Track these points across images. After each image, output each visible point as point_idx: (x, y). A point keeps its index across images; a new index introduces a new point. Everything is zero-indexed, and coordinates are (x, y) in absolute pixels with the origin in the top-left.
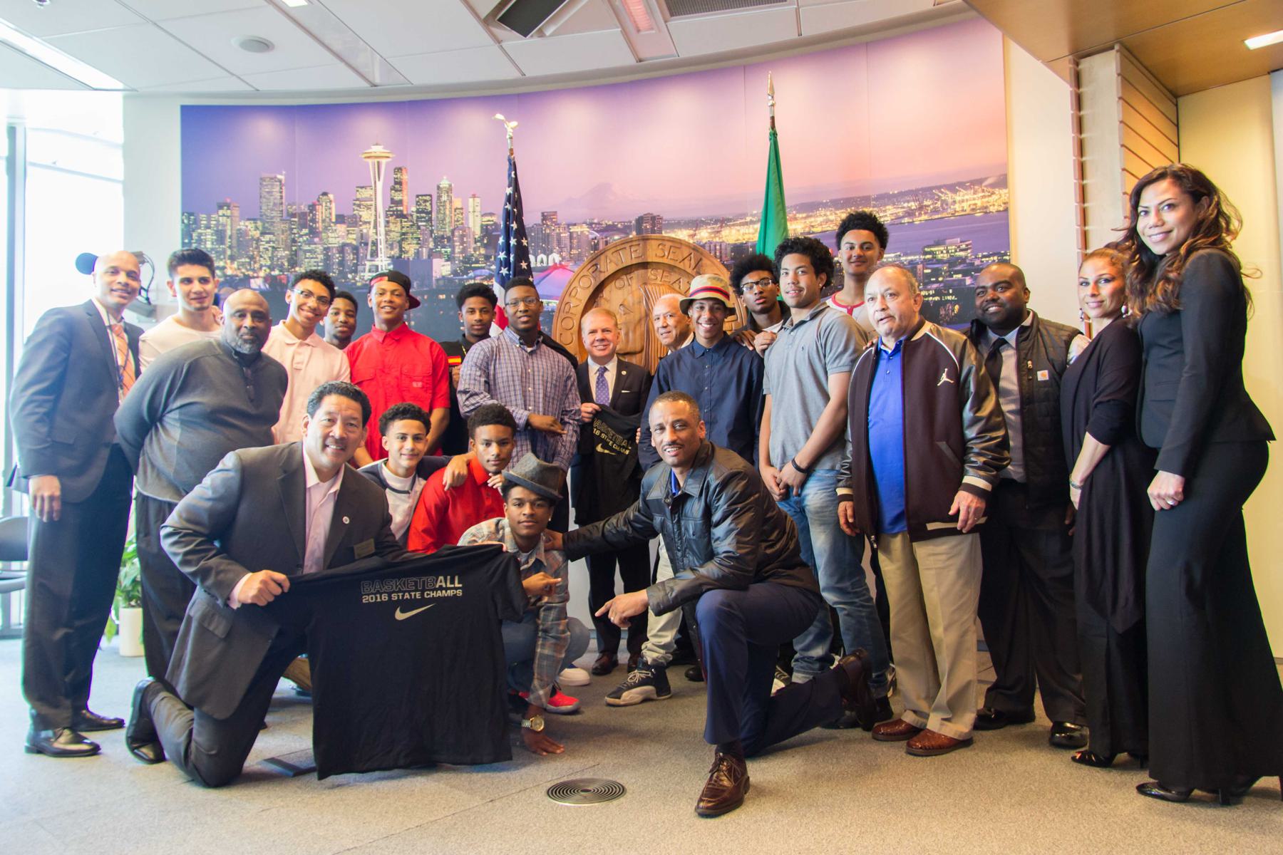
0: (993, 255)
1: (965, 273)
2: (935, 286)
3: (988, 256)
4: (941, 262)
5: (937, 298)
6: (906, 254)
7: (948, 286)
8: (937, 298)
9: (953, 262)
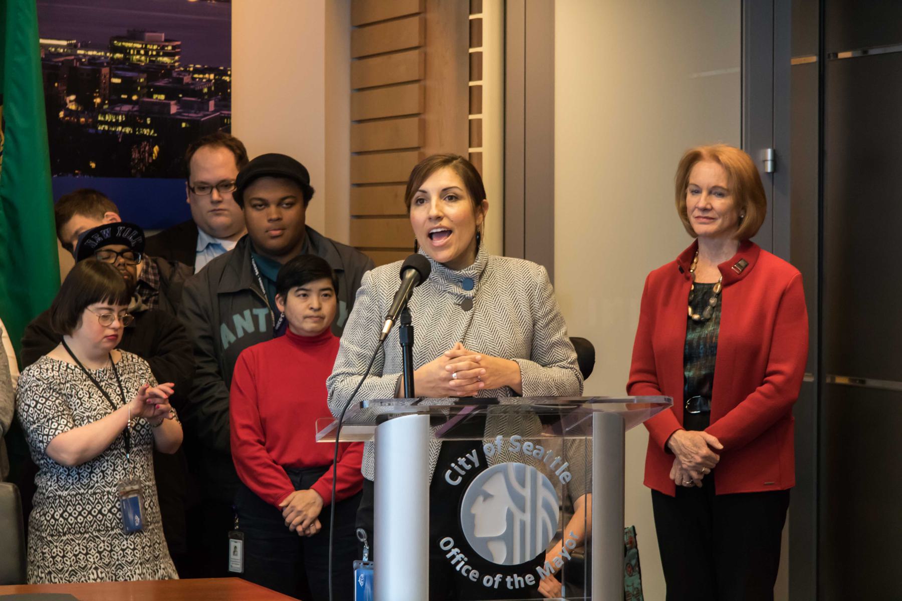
0: (209, 70)
1: (171, 95)
2: (126, 108)
3: (202, 71)
4: (135, 67)
5: (128, 130)
6: (86, 47)
7: (146, 109)
8: (128, 130)
9: (154, 71)
